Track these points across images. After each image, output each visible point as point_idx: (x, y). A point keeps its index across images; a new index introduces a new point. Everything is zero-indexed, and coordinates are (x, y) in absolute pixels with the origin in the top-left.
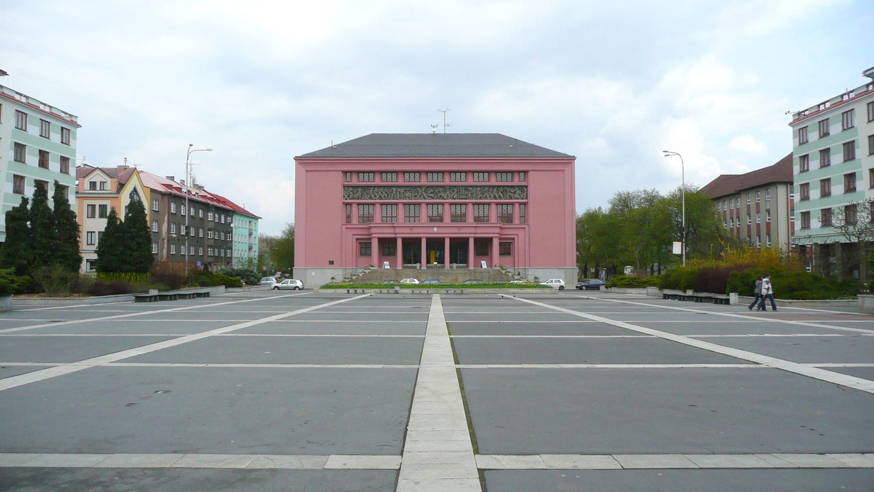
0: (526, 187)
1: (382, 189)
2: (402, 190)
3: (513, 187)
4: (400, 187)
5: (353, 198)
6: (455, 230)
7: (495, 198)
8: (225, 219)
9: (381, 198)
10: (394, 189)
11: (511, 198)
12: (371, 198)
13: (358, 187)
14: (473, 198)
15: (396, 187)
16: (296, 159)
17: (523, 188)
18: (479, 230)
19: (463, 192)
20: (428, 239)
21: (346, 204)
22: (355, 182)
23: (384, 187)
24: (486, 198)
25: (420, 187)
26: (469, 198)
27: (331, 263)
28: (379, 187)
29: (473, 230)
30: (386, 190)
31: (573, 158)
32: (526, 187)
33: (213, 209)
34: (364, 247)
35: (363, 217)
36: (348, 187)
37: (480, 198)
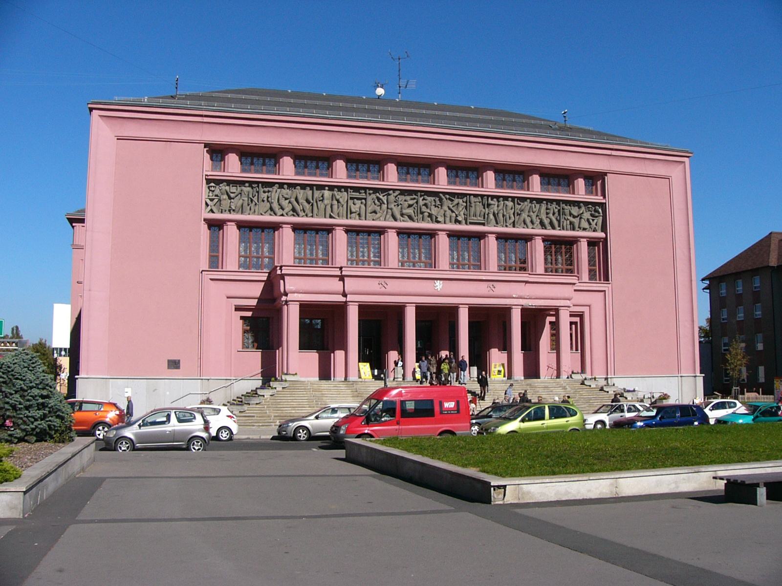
0: (603, 205)
2: (343, 196)
3: (577, 204)
4: (339, 188)
15: (331, 188)
20: (421, 310)
27: (174, 364)
34: (262, 327)
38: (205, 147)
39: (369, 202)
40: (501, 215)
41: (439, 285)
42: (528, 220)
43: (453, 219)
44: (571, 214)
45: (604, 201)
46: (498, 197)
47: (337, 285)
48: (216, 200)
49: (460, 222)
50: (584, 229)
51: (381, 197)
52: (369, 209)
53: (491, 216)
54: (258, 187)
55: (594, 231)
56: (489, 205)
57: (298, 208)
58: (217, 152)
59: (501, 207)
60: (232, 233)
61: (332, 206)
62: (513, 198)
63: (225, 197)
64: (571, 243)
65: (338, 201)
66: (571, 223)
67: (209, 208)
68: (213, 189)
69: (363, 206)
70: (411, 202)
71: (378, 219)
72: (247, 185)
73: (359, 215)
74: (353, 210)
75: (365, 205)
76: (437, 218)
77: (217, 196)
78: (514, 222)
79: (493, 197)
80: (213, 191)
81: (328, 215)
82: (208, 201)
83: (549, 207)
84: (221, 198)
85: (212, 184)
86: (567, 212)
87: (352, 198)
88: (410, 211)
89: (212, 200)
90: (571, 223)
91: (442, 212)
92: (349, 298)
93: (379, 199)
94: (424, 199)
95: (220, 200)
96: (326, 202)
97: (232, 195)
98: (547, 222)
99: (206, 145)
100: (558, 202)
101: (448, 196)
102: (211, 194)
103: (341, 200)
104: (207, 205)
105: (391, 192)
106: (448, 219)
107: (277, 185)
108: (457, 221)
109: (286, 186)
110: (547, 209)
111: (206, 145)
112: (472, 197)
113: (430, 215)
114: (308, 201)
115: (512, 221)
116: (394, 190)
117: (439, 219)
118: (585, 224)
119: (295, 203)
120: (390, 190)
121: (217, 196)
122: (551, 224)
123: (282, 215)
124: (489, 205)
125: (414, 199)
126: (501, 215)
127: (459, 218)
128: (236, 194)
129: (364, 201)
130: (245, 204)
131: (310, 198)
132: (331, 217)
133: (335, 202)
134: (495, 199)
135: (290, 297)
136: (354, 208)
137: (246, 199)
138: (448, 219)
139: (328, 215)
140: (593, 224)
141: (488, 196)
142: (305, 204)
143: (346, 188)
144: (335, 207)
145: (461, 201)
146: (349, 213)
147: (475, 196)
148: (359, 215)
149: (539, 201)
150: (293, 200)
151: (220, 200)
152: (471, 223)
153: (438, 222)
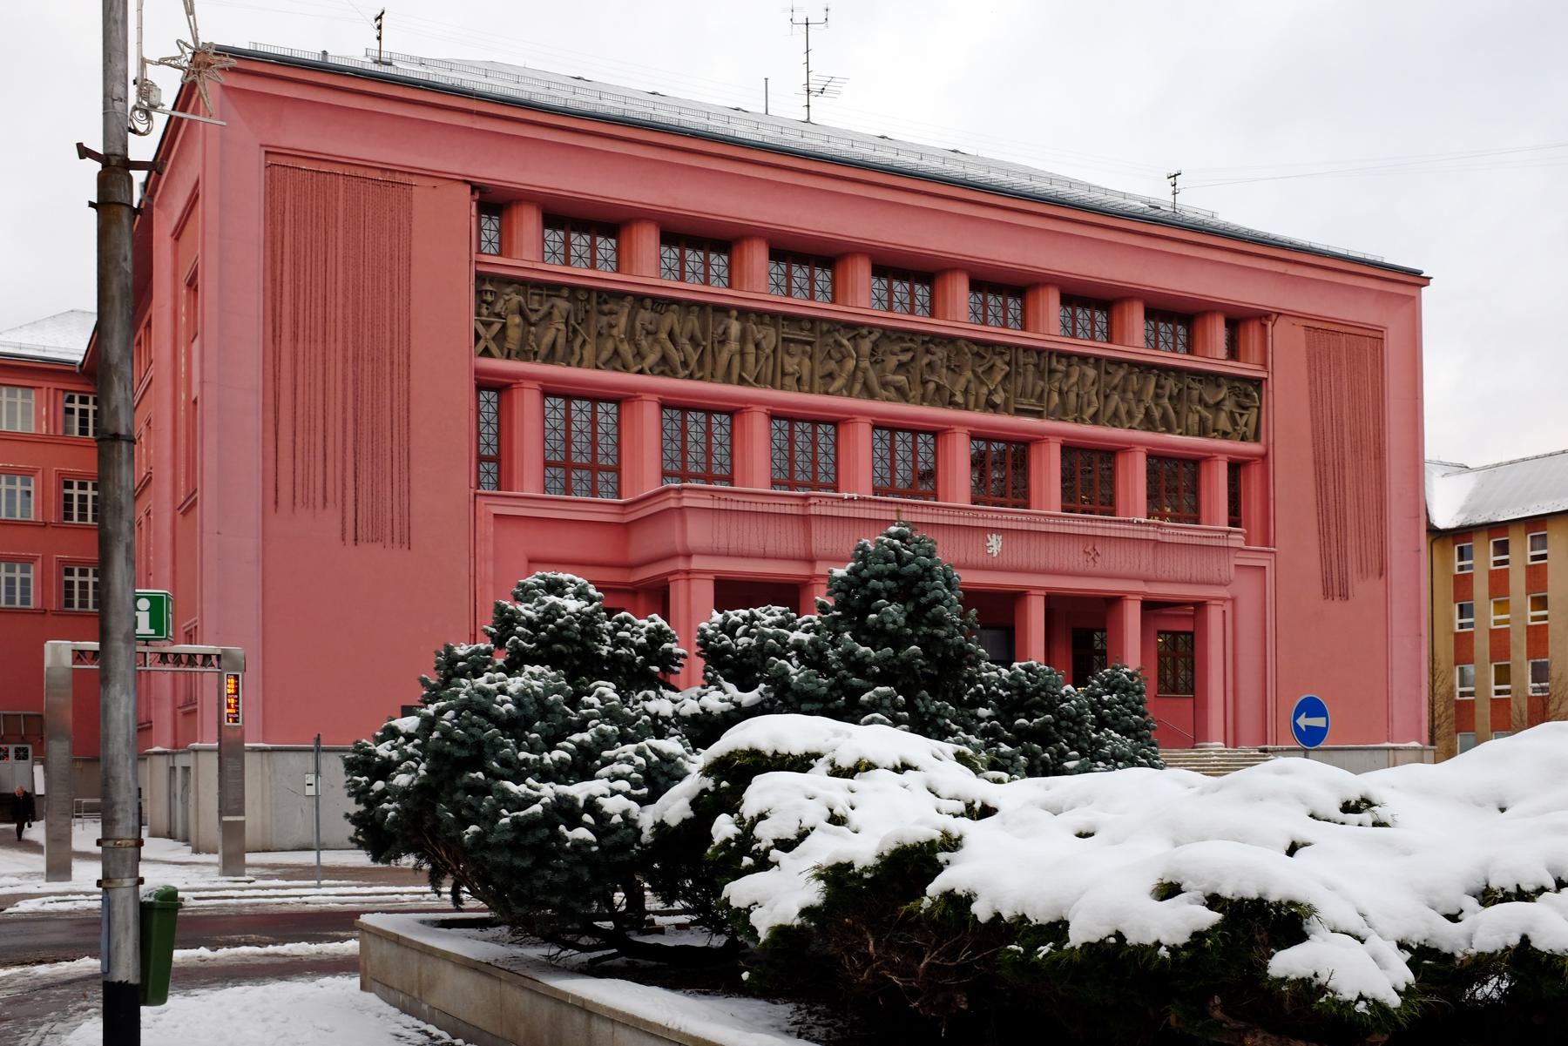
0: (1258, 383)
1: (671, 319)
2: (769, 336)
5: (525, 354)
6: (1072, 557)
7: (1149, 424)
9: (665, 367)
10: (735, 328)
11: (1203, 432)
12: (615, 361)
14: (1062, 413)
15: (743, 313)
17: (1249, 390)
21: (485, 383)
22: (534, 251)
24: (1115, 420)
26: (1051, 415)
28: (661, 303)
30: (693, 322)
31: (1417, 279)
35: (568, 465)
37: (1095, 419)
38: (472, 193)
39: (819, 356)
40: (1072, 396)
43: (983, 400)
44: (1201, 400)
45: (1264, 375)
46: (1068, 356)
47: (787, 539)
48: (497, 327)
50: (1225, 435)
51: (845, 342)
52: (819, 371)
53: (1056, 398)
54: (588, 300)
55: (1242, 439)
56: (1052, 372)
57: (676, 357)
58: (494, 203)
59: (1074, 379)
61: (742, 353)
62: (1098, 359)
63: (517, 319)
64: (1194, 463)
65: (757, 346)
66: (1202, 420)
67: (482, 344)
68: (489, 298)
69: (807, 361)
70: (905, 358)
71: (838, 393)
72: (565, 292)
73: (799, 380)
74: (789, 369)
75: (811, 358)
76: (952, 395)
77: (498, 315)
78: (1096, 413)
79: (1061, 355)
80: (489, 304)
81: (735, 377)
82: (482, 330)
83: (1163, 382)
84: (509, 322)
85: (488, 287)
86: (1195, 394)
87: (784, 339)
88: (901, 379)
89: (488, 325)
90: (1202, 420)
91: (962, 382)
93: (839, 344)
94: (928, 351)
95: (504, 326)
96: (734, 345)
97: (534, 318)
98: (1157, 414)
99: (475, 188)
100: (1179, 372)
101: (975, 348)
102: (484, 311)
103: (764, 344)
104: (478, 337)
105: (865, 331)
106: (972, 399)
107: (630, 298)
108: (992, 406)
109: (648, 303)
110: (1158, 386)
111: (475, 188)
112: (1021, 351)
113: (939, 388)
114: (692, 339)
115: (1092, 410)
116: (871, 328)
117: (959, 399)
118: (1224, 422)
119: (669, 345)
120: (863, 325)
121: (498, 315)
122: (1165, 416)
123: (641, 372)
124: (1052, 372)
125: (908, 350)
126: (1072, 396)
127: (998, 399)
128: (541, 314)
129: (808, 348)
130: (561, 341)
131: (699, 335)
132: (742, 381)
133: (751, 348)
134: (1064, 361)
135: (697, 563)
136: (791, 364)
137: (562, 327)
138: (972, 399)
139: (735, 377)
140: (1242, 422)
141: (1051, 352)
142: (689, 348)
143: (774, 316)
144: (751, 359)
145: (999, 363)
146: (777, 379)
147: (1026, 349)
148: (799, 380)
149: (1146, 368)
150: (664, 336)
151: (504, 326)
152: (1020, 412)
153: (956, 405)
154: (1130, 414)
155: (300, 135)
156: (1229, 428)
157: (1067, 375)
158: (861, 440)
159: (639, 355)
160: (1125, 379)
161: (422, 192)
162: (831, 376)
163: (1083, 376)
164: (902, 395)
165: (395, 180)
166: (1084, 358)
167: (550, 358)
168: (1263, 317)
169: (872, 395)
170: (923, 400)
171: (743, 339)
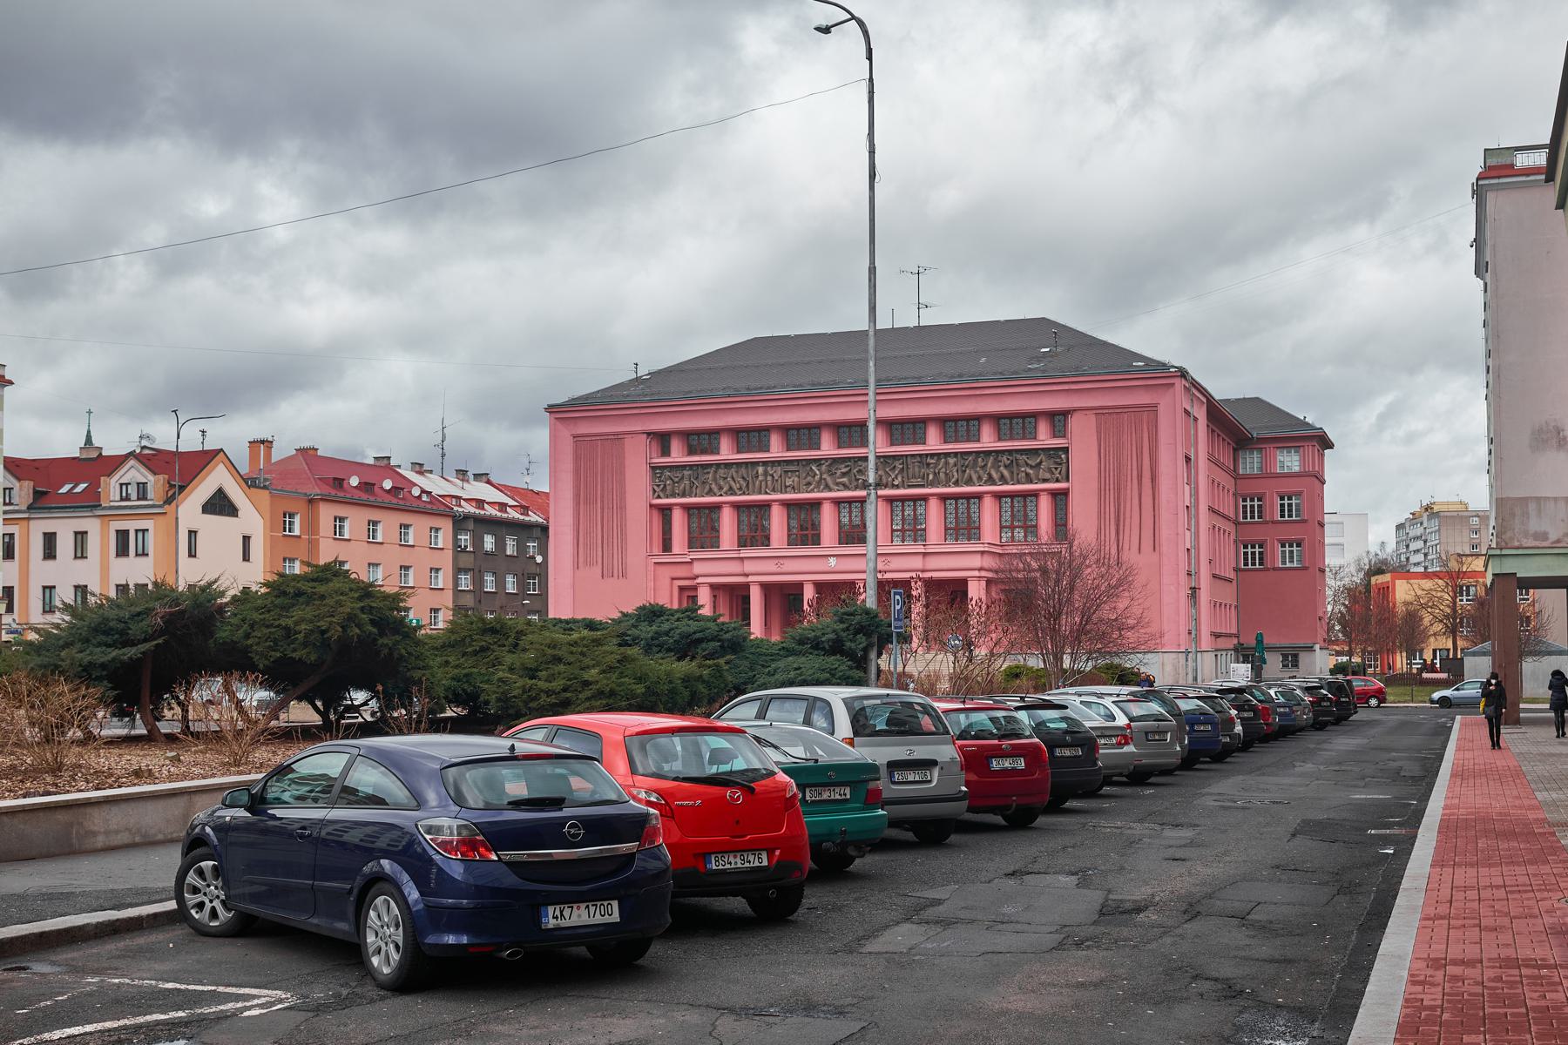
0: (1066, 450)
3: (1035, 452)
5: (673, 495)
7: (991, 481)
8: (521, 547)
9: (731, 492)
10: (761, 469)
12: (710, 492)
13: (684, 467)
15: (765, 463)
16: (551, 409)
18: (933, 563)
19: (915, 468)
23: (739, 465)
24: (969, 482)
25: (818, 461)
26: (932, 484)
28: (728, 465)
29: (917, 563)
30: (743, 471)
32: (1066, 450)
33: (471, 525)
36: (663, 468)
37: (957, 484)
40: (942, 475)
41: (833, 561)
42: (975, 477)
49: (897, 487)
50: (1045, 481)
57: (735, 487)
58: (662, 440)
60: (678, 518)
79: (932, 455)
92: (750, 579)
99: (649, 434)
100: (1010, 452)
122: (1002, 477)
126: (942, 475)
154: (980, 478)
155: (584, 429)
156: (1048, 476)
157: (936, 465)
158: (827, 512)
159: (721, 488)
160: (975, 461)
161: (628, 441)
162: (809, 484)
163: (947, 463)
164: (846, 487)
165: (618, 437)
166: (947, 455)
167: (684, 495)
168: (1065, 413)
169: (830, 490)
170: (856, 488)
171: (766, 473)
